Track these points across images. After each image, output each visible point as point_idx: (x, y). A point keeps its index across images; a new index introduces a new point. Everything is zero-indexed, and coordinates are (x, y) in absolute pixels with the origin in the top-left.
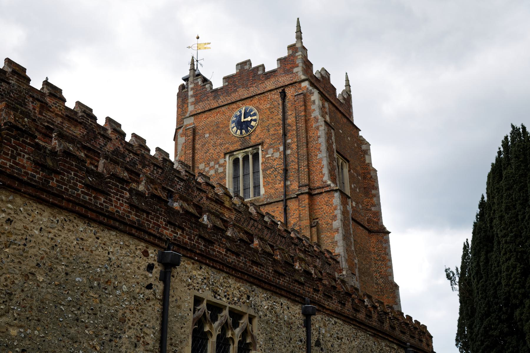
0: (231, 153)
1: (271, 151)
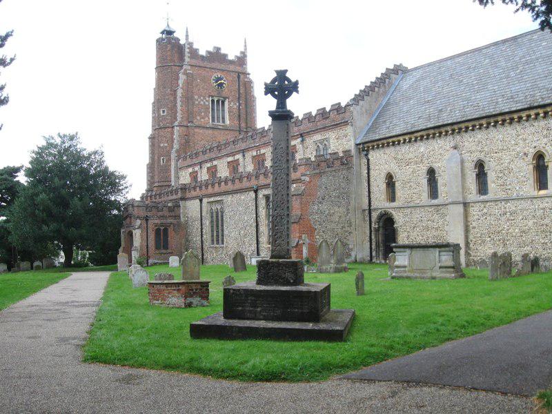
0: (212, 96)
1: (232, 103)
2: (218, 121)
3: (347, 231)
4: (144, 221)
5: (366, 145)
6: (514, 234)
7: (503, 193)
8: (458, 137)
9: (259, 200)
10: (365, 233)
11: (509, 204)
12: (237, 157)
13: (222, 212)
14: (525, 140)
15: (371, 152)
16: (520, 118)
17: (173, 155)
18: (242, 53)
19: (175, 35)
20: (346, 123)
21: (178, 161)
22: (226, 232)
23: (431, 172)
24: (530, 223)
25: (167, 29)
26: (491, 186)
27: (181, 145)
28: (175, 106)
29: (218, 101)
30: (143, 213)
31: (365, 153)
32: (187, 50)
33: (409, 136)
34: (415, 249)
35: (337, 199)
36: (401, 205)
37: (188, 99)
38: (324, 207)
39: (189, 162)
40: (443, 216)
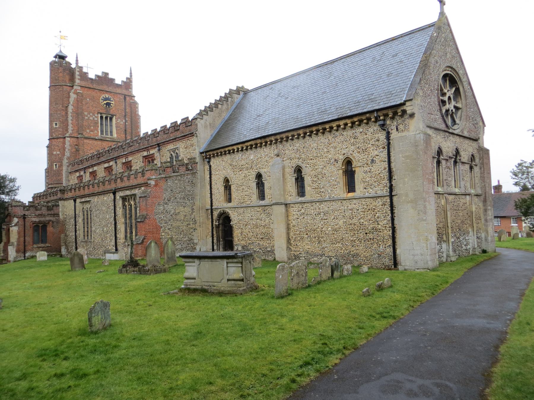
0: (101, 113)
1: (119, 120)
2: (107, 134)
3: (192, 228)
4: (22, 219)
5: (208, 154)
6: (327, 232)
7: (318, 195)
8: (280, 146)
9: (117, 201)
10: (208, 229)
11: (322, 205)
12: (111, 163)
13: (91, 211)
14: (336, 148)
15: (212, 160)
16: (331, 128)
17: (65, 161)
18: (127, 78)
19: (67, 59)
20: (192, 135)
21: (68, 166)
22: (93, 229)
23: (259, 176)
24: (341, 223)
25: (61, 54)
26: (308, 189)
27: (71, 153)
28: (67, 120)
29: (106, 118)
30: (20, 212)
31: (208, 160)
32: (77, 73)
33: (241, 145)
34: (203, 260)
35: (182, 201)
36: (235, 206)
37: (78, 114)
38: (170, 207)
39: (76, 167)
40: (269, 215)
